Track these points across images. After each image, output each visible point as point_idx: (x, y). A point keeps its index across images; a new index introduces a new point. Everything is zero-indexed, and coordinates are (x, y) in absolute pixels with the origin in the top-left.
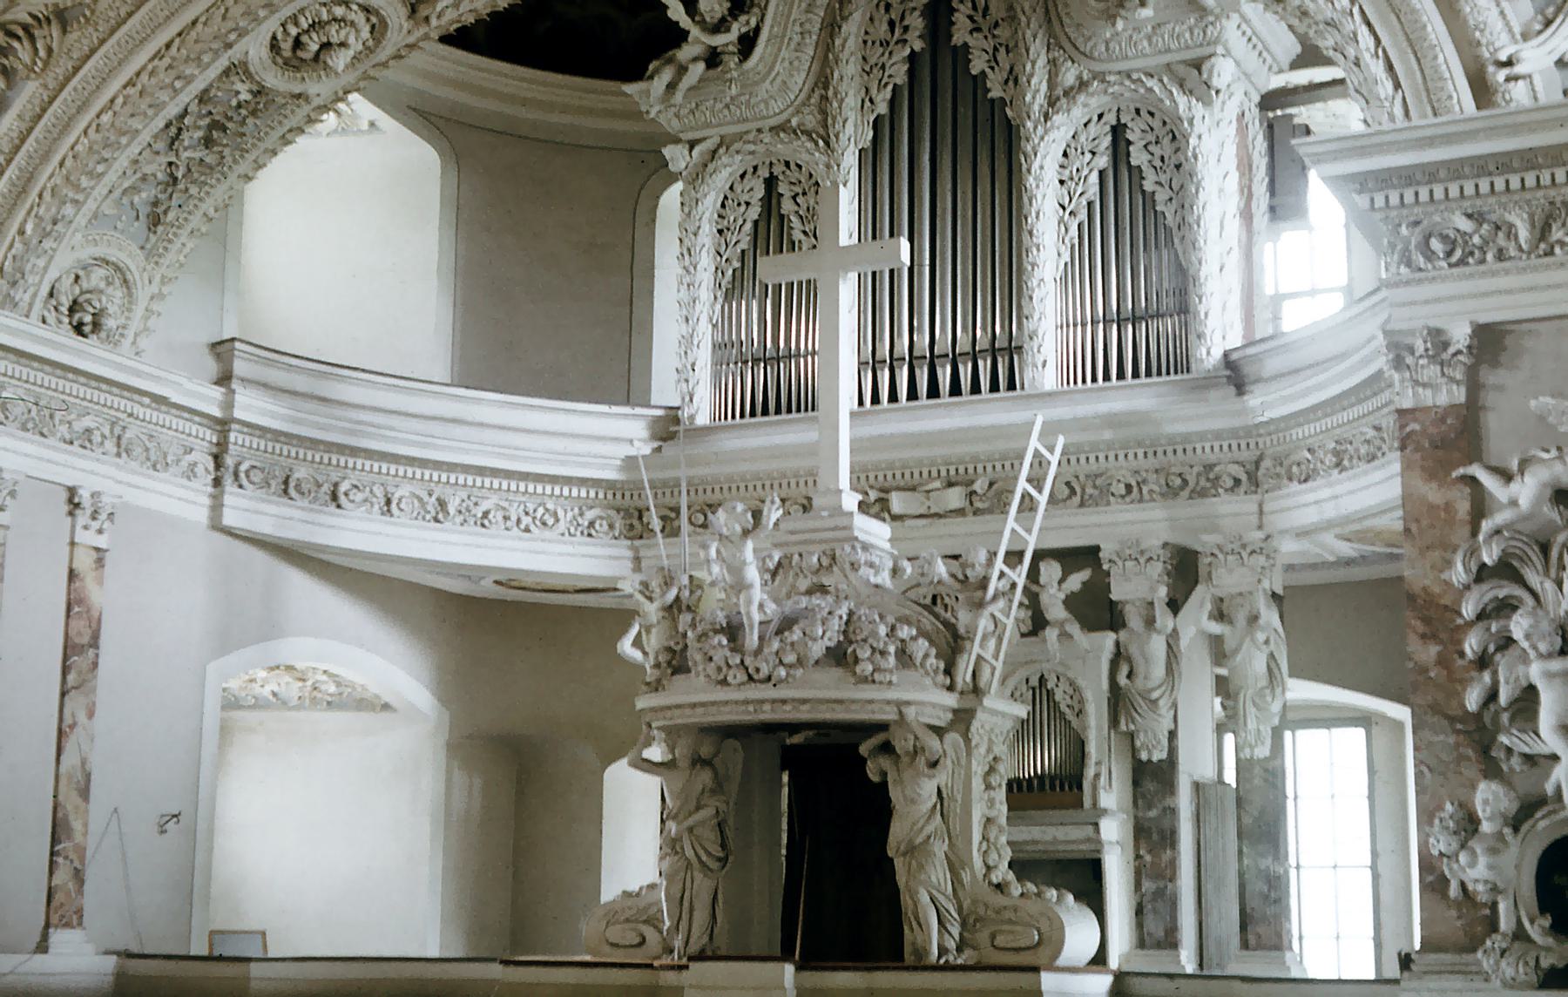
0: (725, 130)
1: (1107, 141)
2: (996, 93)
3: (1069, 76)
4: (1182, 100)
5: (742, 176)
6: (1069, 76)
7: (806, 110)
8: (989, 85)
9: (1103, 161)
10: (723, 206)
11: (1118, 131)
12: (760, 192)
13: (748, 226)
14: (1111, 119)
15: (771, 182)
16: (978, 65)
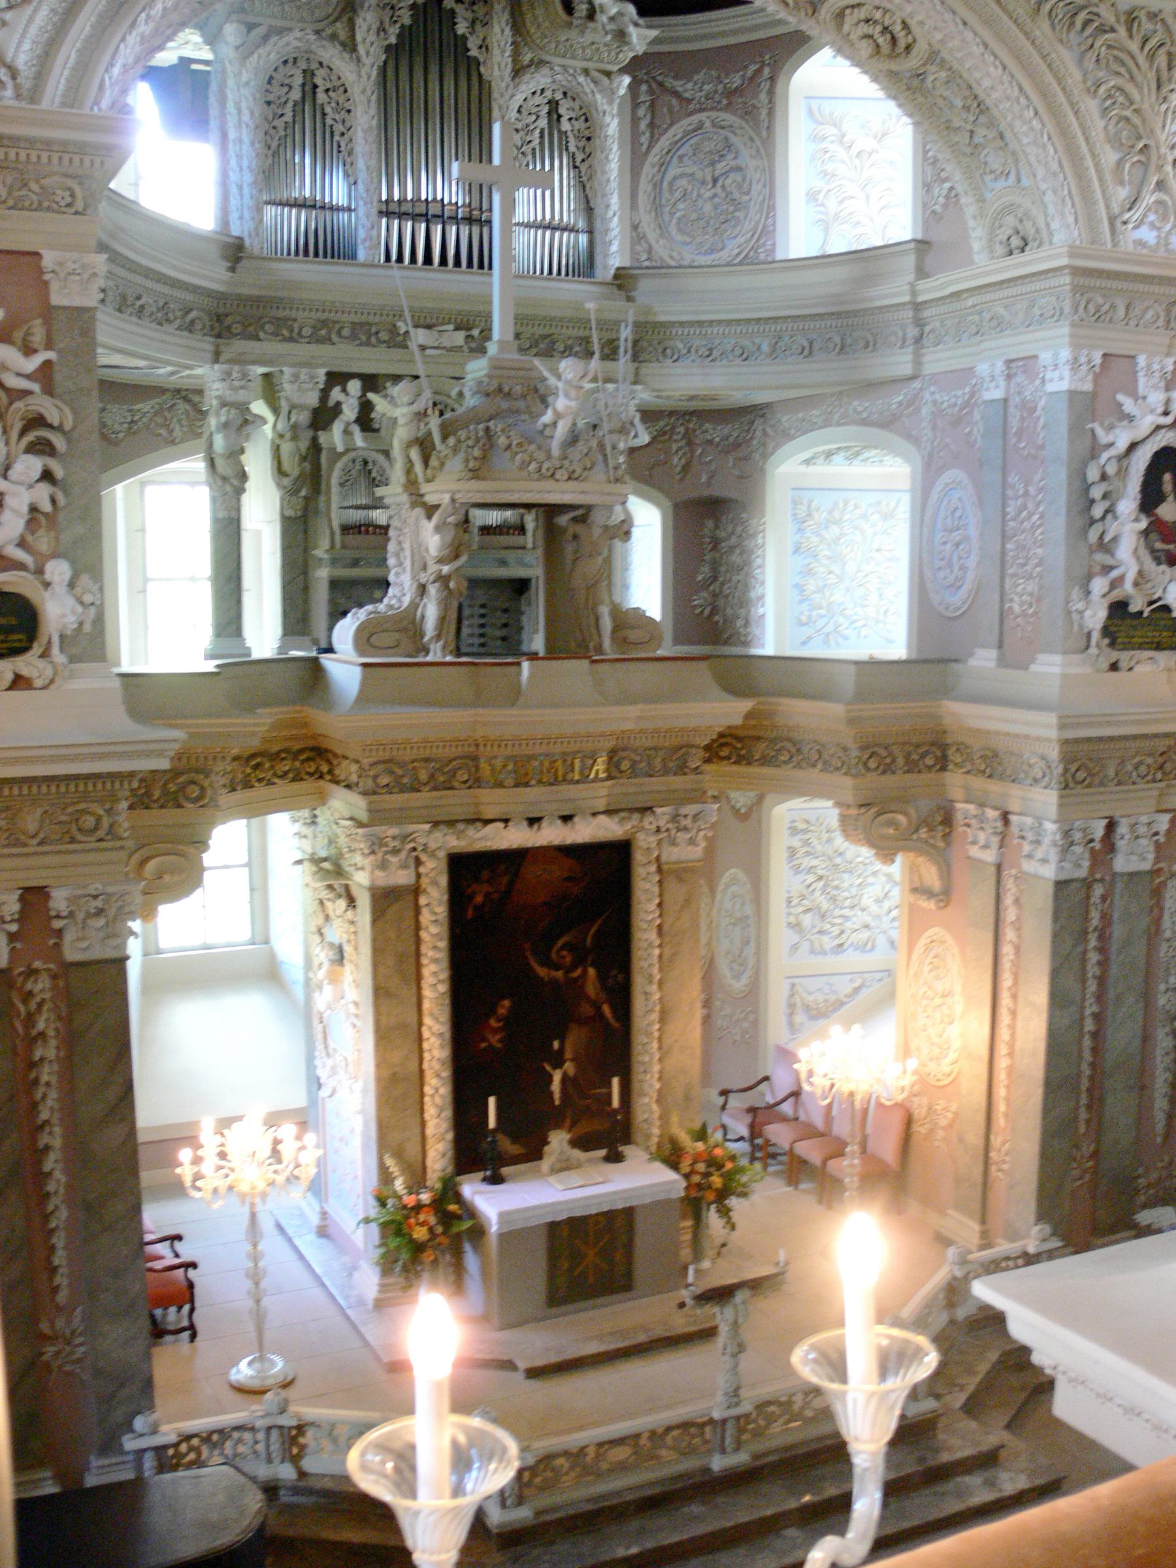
0: (273, 22)
1: (546, 109)
2: (474, 52)
3: (527, 58)
4: (598, 96)
5: (285, 62)
6: (527, 58)
7: (338, 24)
8: (469, 45)
9: (543, 123)
10: (269, 82)
11: (553, 105)
12: (298, 80)
13: (290, 104)
14: (548, 94)
15: (308, 74)
16: (461, 28)
